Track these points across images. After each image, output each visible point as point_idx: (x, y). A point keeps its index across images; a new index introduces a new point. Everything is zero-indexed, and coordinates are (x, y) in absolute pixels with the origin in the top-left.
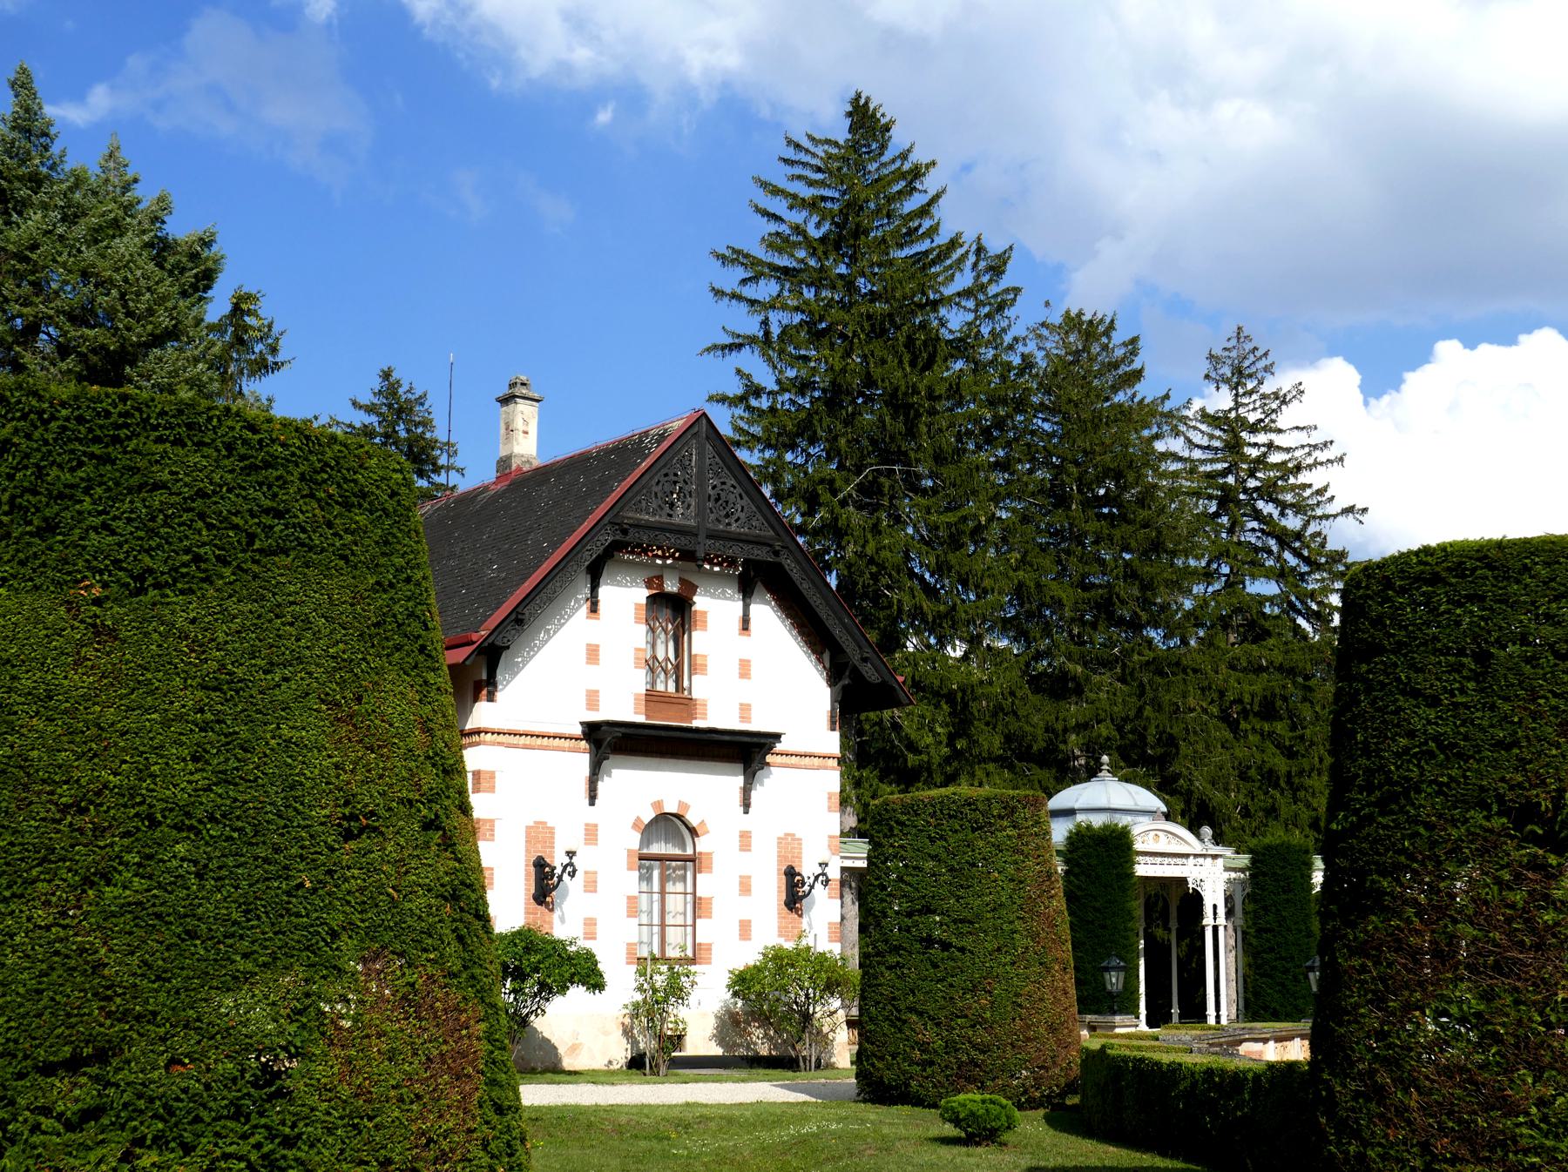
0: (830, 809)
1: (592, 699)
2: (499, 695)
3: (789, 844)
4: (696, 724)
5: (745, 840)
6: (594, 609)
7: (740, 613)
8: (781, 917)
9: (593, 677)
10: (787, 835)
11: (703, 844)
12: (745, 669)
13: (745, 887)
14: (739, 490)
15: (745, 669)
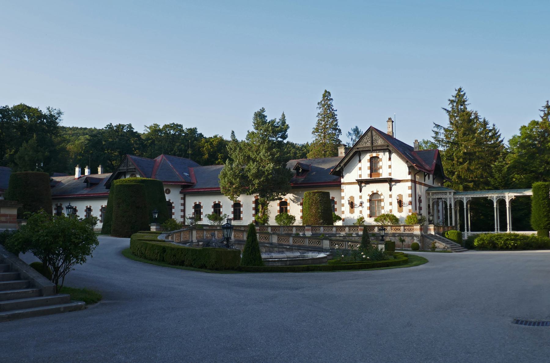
0: (409, 189)
1: (360, 176)
2: (345, 178)
3: (400, 196)
4: (381, 177)
5: (391, 196)
6: (360, 161)
7: (388, 157)
8: (398, 209)
9: (360, 173)
10: (399, 194)
11: (382, 197)
12: (390, 167)
13: (391, 204)
14: (379, 137)
15: (390, 167)
